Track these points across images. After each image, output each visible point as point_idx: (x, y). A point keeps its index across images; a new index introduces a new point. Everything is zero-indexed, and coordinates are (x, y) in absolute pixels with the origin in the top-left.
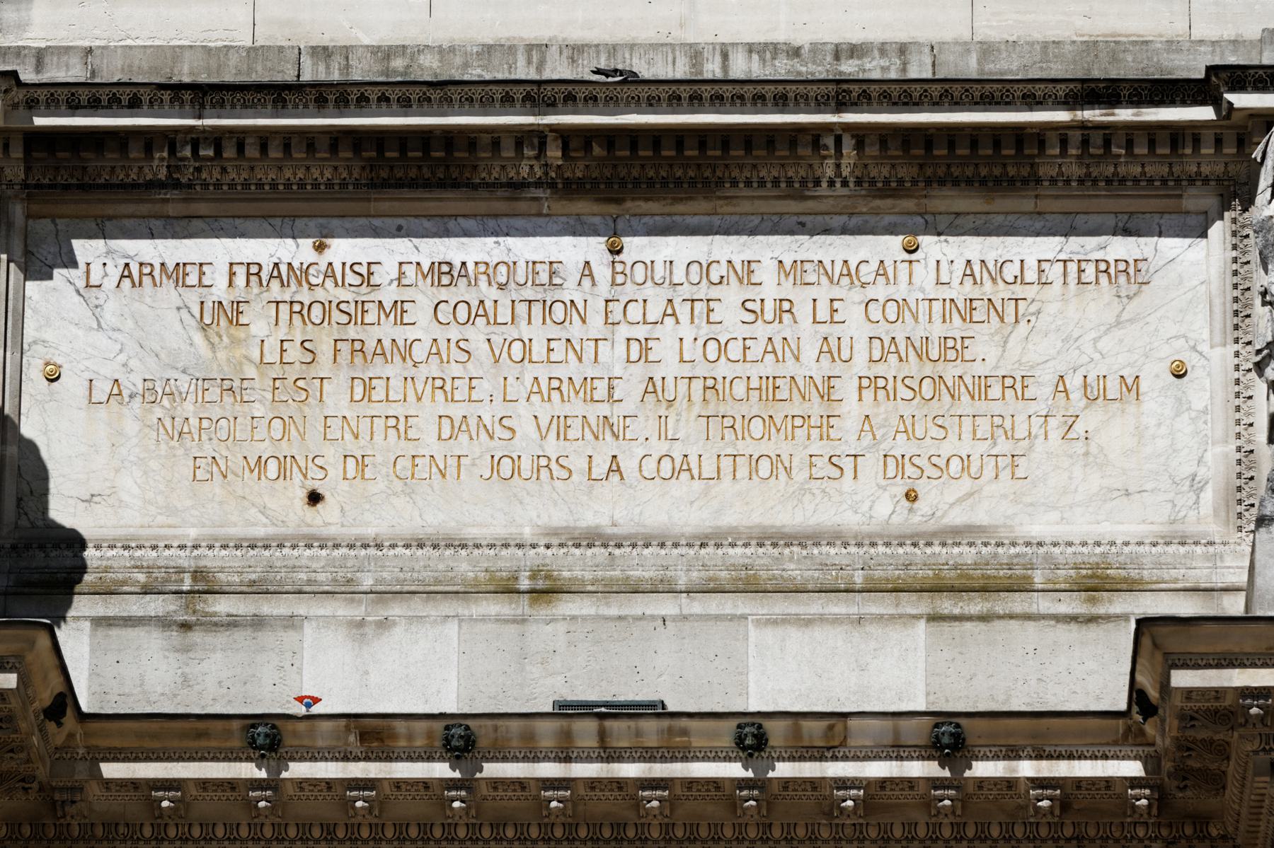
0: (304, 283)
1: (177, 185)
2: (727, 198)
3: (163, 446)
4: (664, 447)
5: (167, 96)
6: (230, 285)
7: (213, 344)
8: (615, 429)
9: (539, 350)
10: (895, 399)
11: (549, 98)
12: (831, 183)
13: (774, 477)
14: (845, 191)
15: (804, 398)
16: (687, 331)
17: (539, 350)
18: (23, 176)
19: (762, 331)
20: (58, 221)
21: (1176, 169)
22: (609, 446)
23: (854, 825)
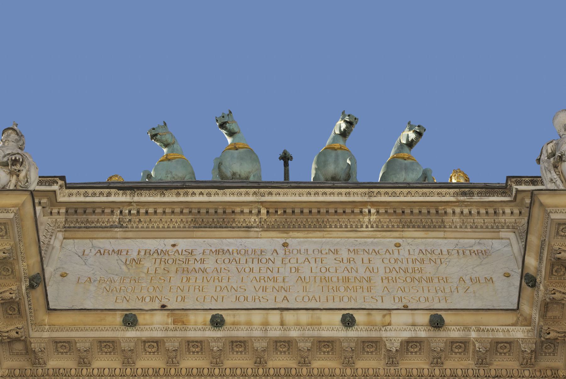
0: (167, 254)
1: (122, 227)
2: (327, 231)
3: (104, 293)
4: (305, 294)
5: (121, 192)
6: (138, 254)
7: (129, 269)
8: (286, 289)
9: (256, 269)
10: (396, 282)
11: (262, 194)
12: (367, 227)
13: (350, 301)
14: (372, 229)
15: (360, 282)
16: (313, 264)
17: (256, 269)
18: (64, 223)
19: (343, 266)
20: (75, 240)
21: (496, 220)
22: (284, 293)
23: (395, 369)
